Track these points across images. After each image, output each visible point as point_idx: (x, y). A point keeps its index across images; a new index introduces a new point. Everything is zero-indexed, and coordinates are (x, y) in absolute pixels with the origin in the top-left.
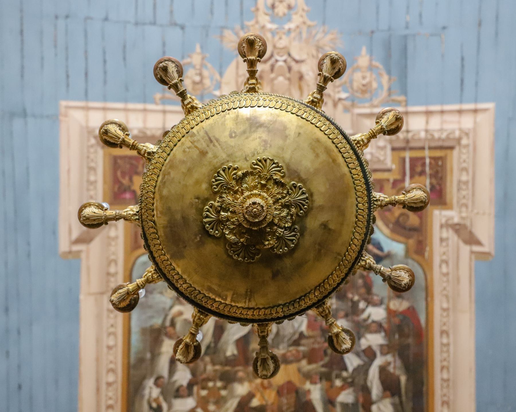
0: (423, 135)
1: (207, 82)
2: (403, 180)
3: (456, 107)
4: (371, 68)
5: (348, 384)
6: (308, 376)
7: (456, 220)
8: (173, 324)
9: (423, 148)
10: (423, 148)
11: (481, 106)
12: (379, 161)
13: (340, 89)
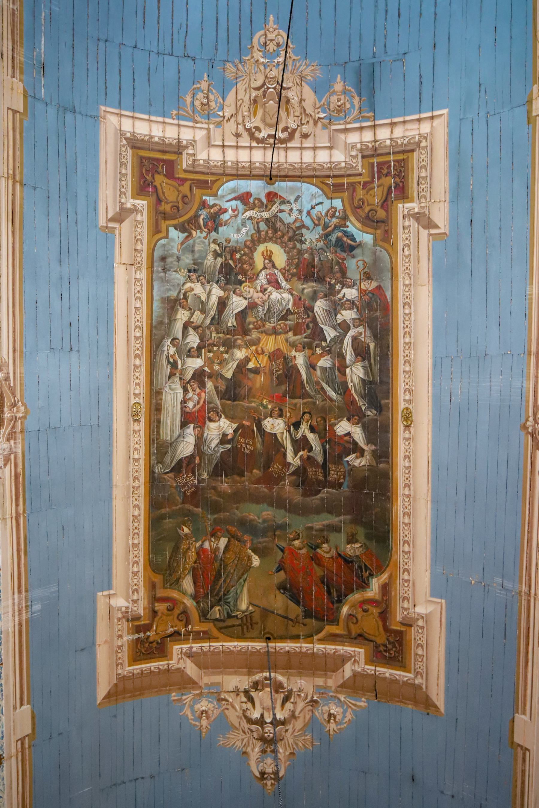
1: (213, 104)
4: (345, 92)
6: (293, 345)
8: (185, 297)
13: (319, 110)
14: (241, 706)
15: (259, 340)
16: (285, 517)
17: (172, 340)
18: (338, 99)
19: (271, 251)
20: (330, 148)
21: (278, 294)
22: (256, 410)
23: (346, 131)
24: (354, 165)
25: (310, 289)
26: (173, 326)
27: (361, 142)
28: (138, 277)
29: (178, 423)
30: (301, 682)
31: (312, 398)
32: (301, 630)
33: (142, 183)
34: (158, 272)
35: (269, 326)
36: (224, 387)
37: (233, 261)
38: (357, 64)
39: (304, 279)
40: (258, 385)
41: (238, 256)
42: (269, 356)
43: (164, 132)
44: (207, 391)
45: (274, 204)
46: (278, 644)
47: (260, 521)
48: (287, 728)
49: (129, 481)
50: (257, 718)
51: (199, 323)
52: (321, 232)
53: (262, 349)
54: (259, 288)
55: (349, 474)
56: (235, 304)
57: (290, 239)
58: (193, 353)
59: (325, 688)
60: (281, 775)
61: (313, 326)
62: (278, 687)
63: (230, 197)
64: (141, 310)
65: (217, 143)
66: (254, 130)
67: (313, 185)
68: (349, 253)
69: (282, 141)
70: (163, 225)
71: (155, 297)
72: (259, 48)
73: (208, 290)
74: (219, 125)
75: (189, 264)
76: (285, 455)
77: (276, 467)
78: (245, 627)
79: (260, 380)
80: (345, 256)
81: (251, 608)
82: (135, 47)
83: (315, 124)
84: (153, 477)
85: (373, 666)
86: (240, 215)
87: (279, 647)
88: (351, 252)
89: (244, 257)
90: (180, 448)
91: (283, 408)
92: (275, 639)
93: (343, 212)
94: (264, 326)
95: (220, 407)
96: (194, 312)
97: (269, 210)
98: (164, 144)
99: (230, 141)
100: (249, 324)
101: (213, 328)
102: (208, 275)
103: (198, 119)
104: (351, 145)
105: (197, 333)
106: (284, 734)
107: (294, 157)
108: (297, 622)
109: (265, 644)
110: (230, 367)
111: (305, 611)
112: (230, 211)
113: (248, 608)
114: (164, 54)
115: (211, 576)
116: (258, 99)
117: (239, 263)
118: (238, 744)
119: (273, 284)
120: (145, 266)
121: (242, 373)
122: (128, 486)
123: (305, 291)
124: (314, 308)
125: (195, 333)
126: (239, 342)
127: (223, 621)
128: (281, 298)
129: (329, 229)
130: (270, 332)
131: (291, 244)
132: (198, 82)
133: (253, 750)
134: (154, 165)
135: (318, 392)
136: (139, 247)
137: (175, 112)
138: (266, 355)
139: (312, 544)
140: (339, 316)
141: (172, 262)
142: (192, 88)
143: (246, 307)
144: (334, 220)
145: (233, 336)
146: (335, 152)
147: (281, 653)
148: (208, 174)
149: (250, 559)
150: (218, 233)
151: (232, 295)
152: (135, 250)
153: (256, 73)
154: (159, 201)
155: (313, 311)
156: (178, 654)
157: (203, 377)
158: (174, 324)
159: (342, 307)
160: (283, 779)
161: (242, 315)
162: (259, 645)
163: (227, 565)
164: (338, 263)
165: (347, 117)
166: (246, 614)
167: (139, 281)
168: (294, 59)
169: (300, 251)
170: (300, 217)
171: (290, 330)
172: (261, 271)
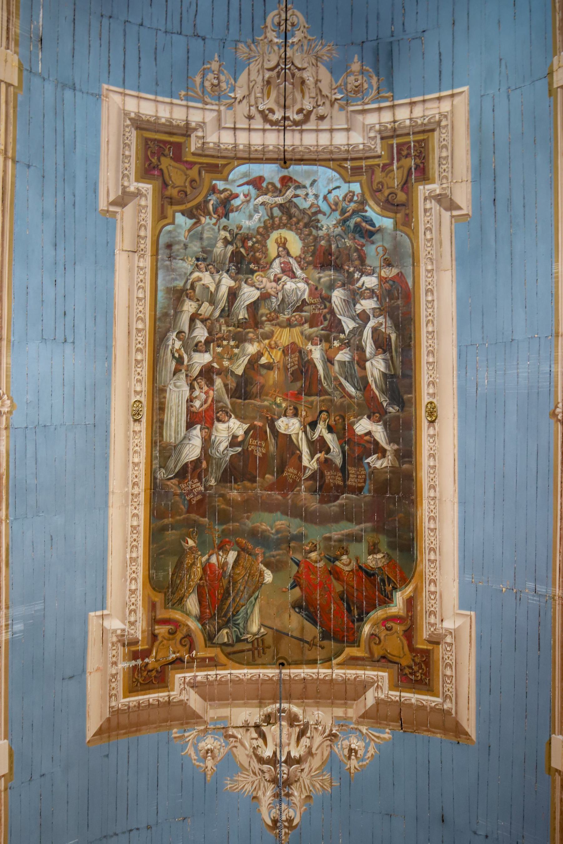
0: (408, 122)
1: (224, 85)
2: (392, 164)
3: (436, 95)
4: (362, 72)
5: (346, 344)
6: (309, 338)
7: (438, 192)
8: (193, 287)
9: (408, 134)
10: (408, 134)
11: (456, 91)
12: (371, 149)
13: (336, 91)
14: (251, 743)
15: (272, 333)
16: (301, 526)
17: (178, 333)
18: (355, 79)
19: (285, 239)
20: (348, 130)
21: (292, 283)
22: (269, 409)
23: (363, 112)
24: (373, 147)
25: (327, 278)
26: (179, 318)
27: (380, 123)
28: (141, 265)
29: (183, 424)
30: (318, 714)
31: (330, 395)
32: (319, 654)
33: (146, 166)
34: (163, 260)
35: (283, 317)
36: (235, 385)
38: (375, 43)
39: (321, 267)
40: (271, 382)
41: (250, 243)
42: (283, 351)
43: (171, 113)
44: (215, 388)
45: (289, 189)
46: (292, 671)
47: (273, 531)
48: (302, 767)
49: (128, 487)
50: (269, 756)
51: (207, 315)
52: (339, 217)
53: (276, 343)
54: (272, 278)
55: (370, 479)
56: (246, 295)
57: (306, 225)
58: (201, 348)
59: (345, 719)
60: (295, 823)
61: (330, 319)
62: (293, 720)
63: (242, 181)
64: (143, 301)
65: (228, 125)
66: (267, 112)
67: (330, 168)
68: (368, 239)
69: (296, 123)
70: (170, 210)
71: (160, 287)
72: (273, 28)
74: (230, 106)
75: (198, 252)
76: (300, 458)
77: (290, 471)
78: (256, 652)
79: (274, 376)
80: (364, 242)
81: (262, 630)
82: (142, 25)
83: (332, 105)
84: (155, 483)
85: (397, 691)
86: (252, 200)
87: (293, 674)
88: (370, 238)
89: (257, 245)
90: (186, 451)
91: (298, 406)
92: (289, 664)
93: (361, 196)
94: (278, 317)
95: (230, 406)
96: (202, 303)
97: (283, 196)
98: (171, 125)
99: (243, 124)
100: (262, 316)
101: (222, 320)
102: (217, 264)
103: (208, 100)
104: (369, 127)
105: (205, 326)
106: (299, 774)
107: (309, 140)
108: (313, 645)
109: (277, 671)
110: (241, 362)
111: (323, 632)
112: (242, 197)
113: (259, 630)
114: (172, 33)
115: (218, 594)
116: (271, 80)
117: (251, 251)
118: (248, 787)
119: (287, 273)
120: (149, 253)
121: (254, 370)
122: (127, 493)
123: (322, 280)
124: (331, 297)
125: (203, 326)
126: (251, 335)
127: (232, 645)
128: (296, 288)
130: (285, 324)
131: (306, 231)
132: (208, 62)
133: (264, 794)
134: (160, 147)
135: (336, 389)
136: (142, 233)
137: (183, 93)
138: (280, 349)
139: (330, 556)
140: (358, 306)
141: (178, 250)
142: (202, 68)
143: (258, 298)
144: (352, 205)
145: (245, 329)
146: (353, 134)
147: (296, 680)
148: (218, 157)
149: (261, 574)
151: (244, 285)
152: (138, 236)
153: (270, 53)
154: (165, 185)
155: (330, 302)
156: (180, 684)
157: (212, 374)
158: (180, 316)
159: (361, 296)
160: (298, 827)
161: (254, 307)
162: (271, 672)
163: (237, 582)
164: (357, 250)
165: (365, 97)
166: (257, 637)
167: (142, 269)
168: (309, 40)
169: (316, 238)
170: (316, 202)
171: (306, 322)
172: (275, 259)
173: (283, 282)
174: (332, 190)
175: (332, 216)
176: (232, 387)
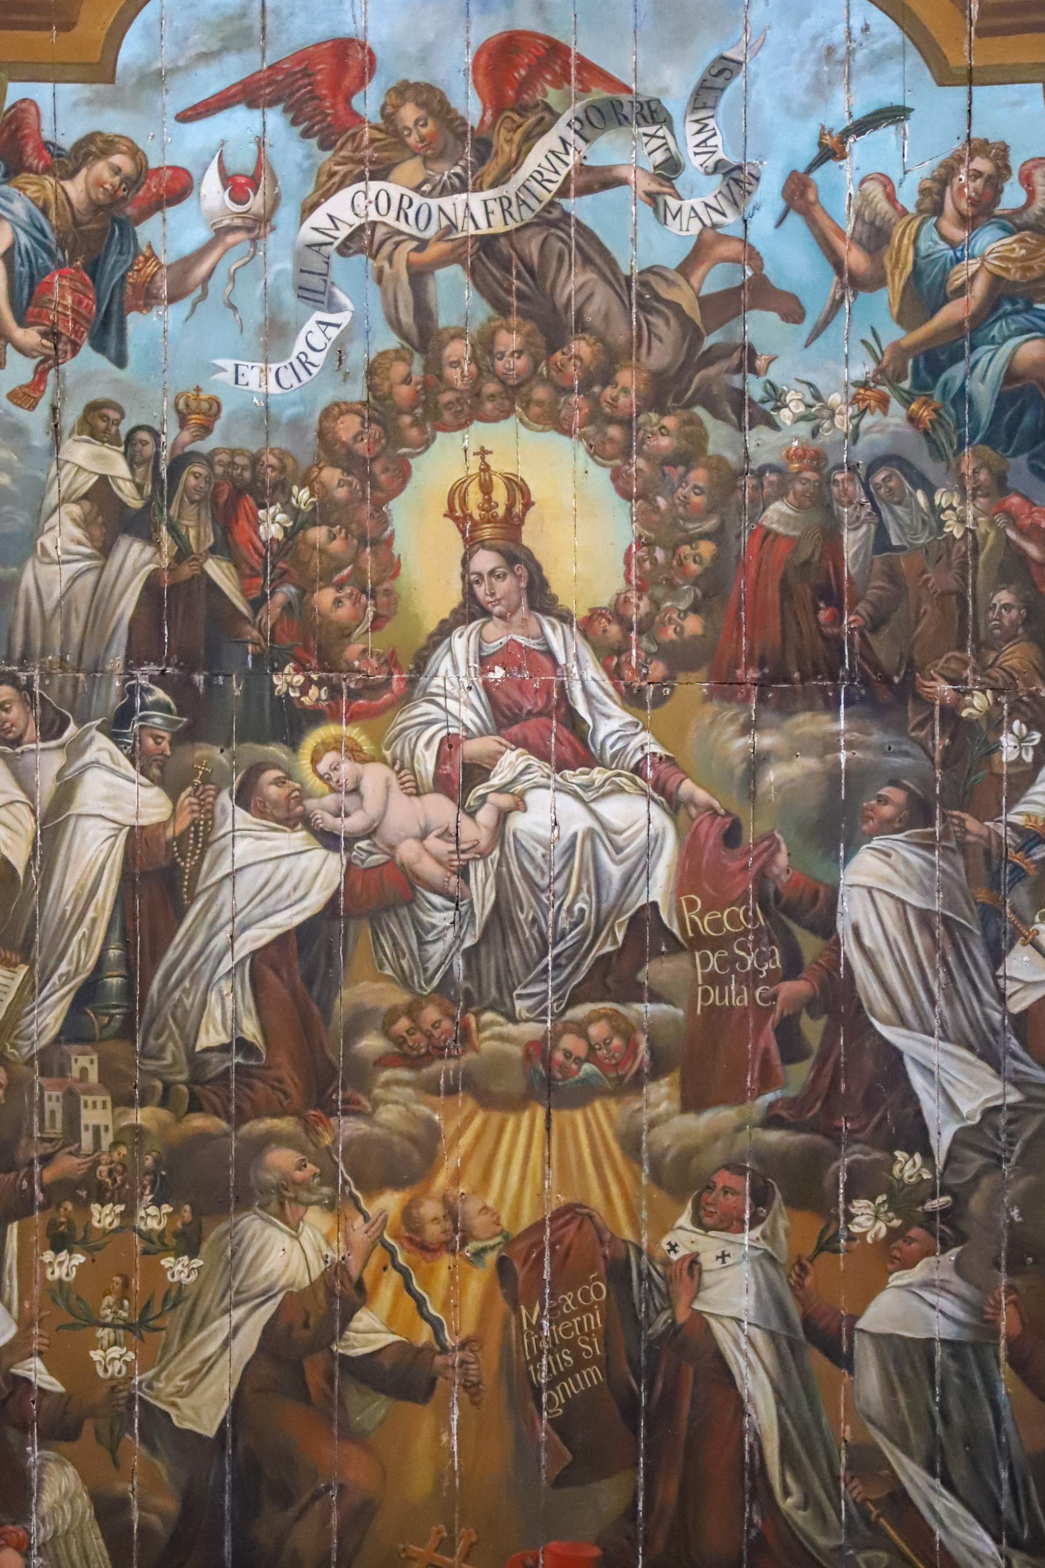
19: (517, 487)
21: (568, 805)
25: (807, 764)
36: (169, 1504)
37: (237, 562)
39: (763, 684)
44: (38, 1532)
45: (541, 128)
52: (892, 334)
54: (427, 762)
56: (248, 883)
61: (829, 1036)
73: (46, 785)
86: (287, 213)
89: (318, 534)
94: (464, 1037)
100: (357, 1025)
102: (46, 674)
121: (304, 1395)
123: (772, 776)
128: (590, 833)
129: (952, 312)
130: (513, 1083)
143: (332, 904)
145: (241, 1118)
150: (120, 361)
171: (658, 1069)
172: (445, 630)
173: (501, 790)
174: (846, 133)
175: (842, 320)
176: (154, 1519)
